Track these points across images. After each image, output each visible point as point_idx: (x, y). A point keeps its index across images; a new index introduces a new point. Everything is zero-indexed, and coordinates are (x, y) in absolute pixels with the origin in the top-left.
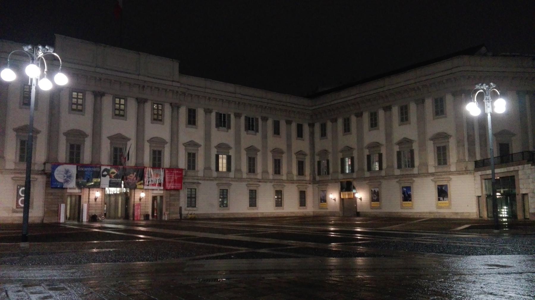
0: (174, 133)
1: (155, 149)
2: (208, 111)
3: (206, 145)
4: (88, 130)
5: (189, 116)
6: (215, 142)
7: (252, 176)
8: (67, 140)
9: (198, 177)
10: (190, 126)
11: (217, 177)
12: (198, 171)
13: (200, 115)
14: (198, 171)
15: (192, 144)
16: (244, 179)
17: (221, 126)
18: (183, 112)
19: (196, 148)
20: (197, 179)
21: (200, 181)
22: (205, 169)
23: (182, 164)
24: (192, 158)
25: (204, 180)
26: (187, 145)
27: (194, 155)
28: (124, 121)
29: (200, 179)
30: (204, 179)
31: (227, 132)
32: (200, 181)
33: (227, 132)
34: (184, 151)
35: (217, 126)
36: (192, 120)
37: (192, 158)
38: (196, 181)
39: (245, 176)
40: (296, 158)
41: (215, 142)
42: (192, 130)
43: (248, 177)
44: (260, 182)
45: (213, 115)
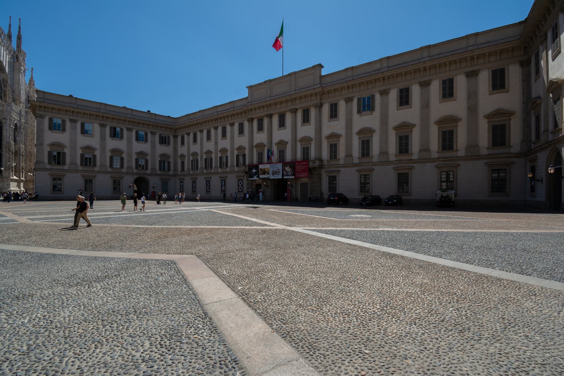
0: (319, 130)
1: (305, 146)
2: (349, 100)
3: (346, 134)
4: (265, 141)
5: (331, 111)
6: (356, 129)
7: (404, 157)
8: (257, 151)
9: (339, 164)
10: (332, 120)
11: (359, 163)
12: (339, 160)
13: (342, 106)
14: (339, 160)
15: (334, 136)
16: (392, 161)
17: (364, 110)
18: (326, 109)
19: (338, 139)
20: (338, 167)
21: (340, 169)
22: (346, 156)
23: (325, 154)
24: (333, 149)
25: (344, 167)
26: (329, 137)
27: (335, 145)
28: (285, 130)
29: (341, 167)
30: (344, 166)
31: (372, 114)
32: (340, 169)
33: (372, 114)
34: (327, 143)
35: (359, 112)
36: (334, 114)
37: (333, 149)
38: (336, 169)
39: (392, 158)
40: (488, 122)
41: (356, 128)
42: (334, 123)
43: (397, 159)
44: (414, 163)
45: (355, 102)
